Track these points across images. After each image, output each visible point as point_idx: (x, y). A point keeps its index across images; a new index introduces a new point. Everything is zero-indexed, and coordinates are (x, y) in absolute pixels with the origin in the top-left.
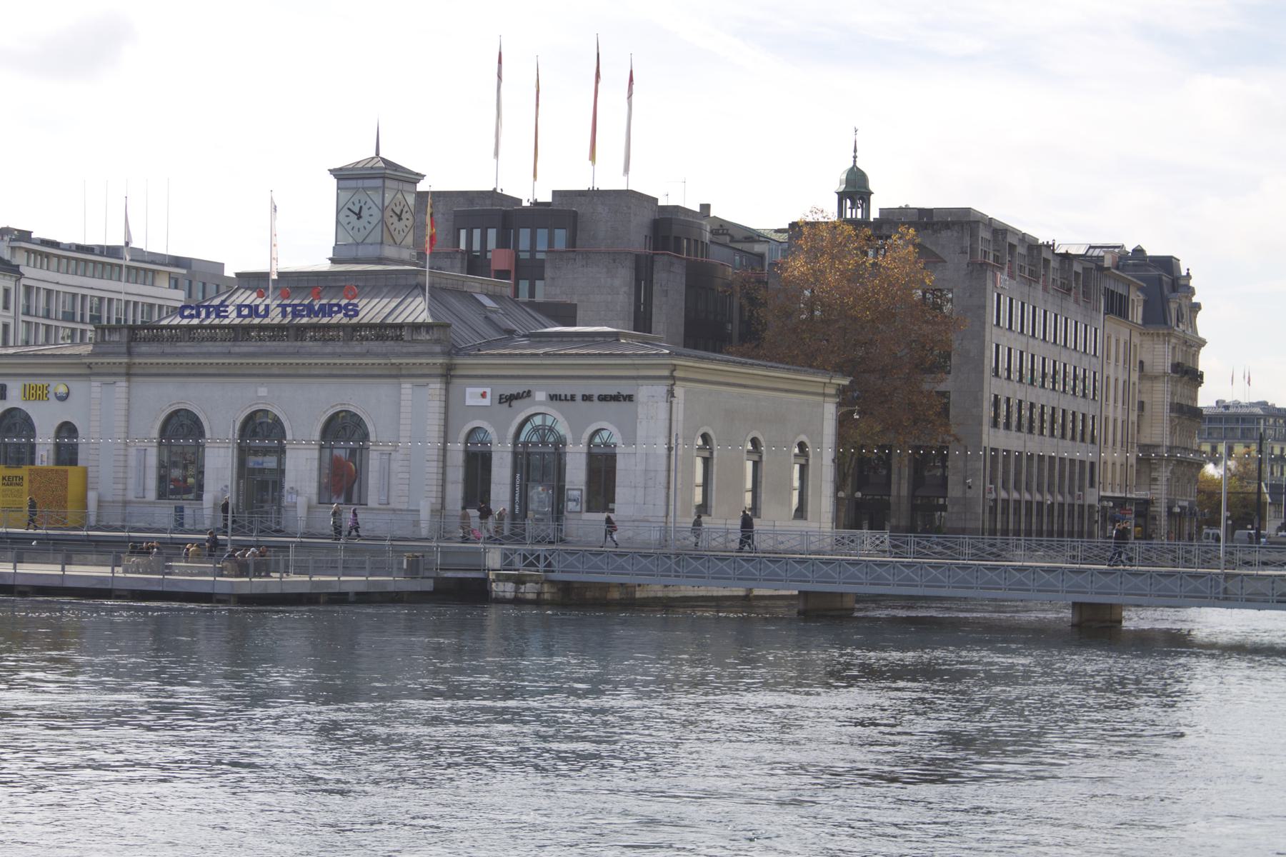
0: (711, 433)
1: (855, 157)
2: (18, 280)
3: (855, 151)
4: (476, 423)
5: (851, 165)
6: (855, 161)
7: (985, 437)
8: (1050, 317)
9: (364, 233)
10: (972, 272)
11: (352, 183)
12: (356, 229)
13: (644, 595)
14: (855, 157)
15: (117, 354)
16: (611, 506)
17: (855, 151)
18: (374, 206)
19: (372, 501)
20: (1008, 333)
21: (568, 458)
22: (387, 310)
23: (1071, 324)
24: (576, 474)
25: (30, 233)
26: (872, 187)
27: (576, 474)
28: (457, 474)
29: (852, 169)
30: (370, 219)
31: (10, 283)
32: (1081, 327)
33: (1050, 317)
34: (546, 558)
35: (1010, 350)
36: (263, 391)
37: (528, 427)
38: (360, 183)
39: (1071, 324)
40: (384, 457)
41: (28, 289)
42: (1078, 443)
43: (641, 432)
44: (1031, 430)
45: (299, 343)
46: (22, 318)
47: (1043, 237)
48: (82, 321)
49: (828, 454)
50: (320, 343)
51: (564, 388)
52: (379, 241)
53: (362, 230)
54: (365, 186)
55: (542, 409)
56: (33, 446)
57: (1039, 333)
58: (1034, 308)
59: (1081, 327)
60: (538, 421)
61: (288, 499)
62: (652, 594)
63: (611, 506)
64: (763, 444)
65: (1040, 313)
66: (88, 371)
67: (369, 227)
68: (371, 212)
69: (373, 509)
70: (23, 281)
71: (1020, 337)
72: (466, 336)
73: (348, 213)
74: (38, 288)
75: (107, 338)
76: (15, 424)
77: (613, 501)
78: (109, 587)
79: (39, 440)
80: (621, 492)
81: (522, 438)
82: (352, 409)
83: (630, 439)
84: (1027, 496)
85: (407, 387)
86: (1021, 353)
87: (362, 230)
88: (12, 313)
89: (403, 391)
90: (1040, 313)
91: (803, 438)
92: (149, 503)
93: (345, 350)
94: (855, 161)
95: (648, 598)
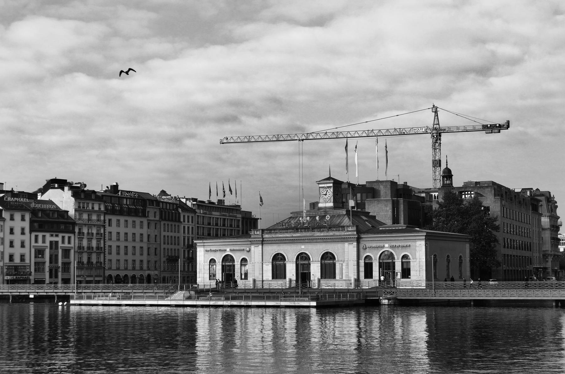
0: (450, 255)
1: (447, 165)
2: (195, 214)
3: (447, 163)
4: (368, 254)
5: (446, 167)
6: (447, 166)
7: (502, 251)
8: (517, 213)
10: (495, 201)
12: (325, 199)
14: (447, 165)
15: (259, 238)
16: (409, 277)
17: (447, 163)
18: (330, 192)
19: (338, 277)
20: (506, 219)
21: (396, 263)
23: (523, 215)
24: (398, 268)
26: (452, 174)
27: (398, 268)
28: (362, 269)
29: (446, 168)
30: (330, 195)
31: (193, 215)
32: (525, 215)
33: (517, 213)
34: (396, 293)
35: (507, 224)
36: (303, 247)
37: (383, 255)
39: (523, 215)
40: (341, 265)
41: (198, 216)
42: (527, 251)
43: (417, 254)
44: (528, 250)
45: (313, 233)
46: (197, 225)
47: (511, 188)
48: (213, 225)
49: (468, 259)
50: (319, 232)
51: (394, 244)
53: (327, 198)
55: (387, 249)
56: (234, 266)
57: (515, 218)
58: (513, 211)
59: (525, 215)
60: (386, 253)
61: (312, 278)
63: (409, 277)
64: (463, 257)
65: (514, 212)
66: (250, 243)
68: (329, 193)
69: (337, 280)
70: (197, 214)
71: (510, 220)
72: (535, 249)
74: (201, 216)
75: (255, 233)
76: (228, 259)
77: (410, 275)
78: (279, 305)
79: (236, 263)
80: (412, 273)
81: (381, 258)
82: (330, 251)
83: (415, 258)
84: (514, 268)
85: (346, 244)
86: (510, 224)
87: (327, 198)
88: (194, 224)
89: (345, 246)
90: (514, 212)
91: (461, 254)
92: (270, 280)
93: (327, 234)
94: (447, 166)
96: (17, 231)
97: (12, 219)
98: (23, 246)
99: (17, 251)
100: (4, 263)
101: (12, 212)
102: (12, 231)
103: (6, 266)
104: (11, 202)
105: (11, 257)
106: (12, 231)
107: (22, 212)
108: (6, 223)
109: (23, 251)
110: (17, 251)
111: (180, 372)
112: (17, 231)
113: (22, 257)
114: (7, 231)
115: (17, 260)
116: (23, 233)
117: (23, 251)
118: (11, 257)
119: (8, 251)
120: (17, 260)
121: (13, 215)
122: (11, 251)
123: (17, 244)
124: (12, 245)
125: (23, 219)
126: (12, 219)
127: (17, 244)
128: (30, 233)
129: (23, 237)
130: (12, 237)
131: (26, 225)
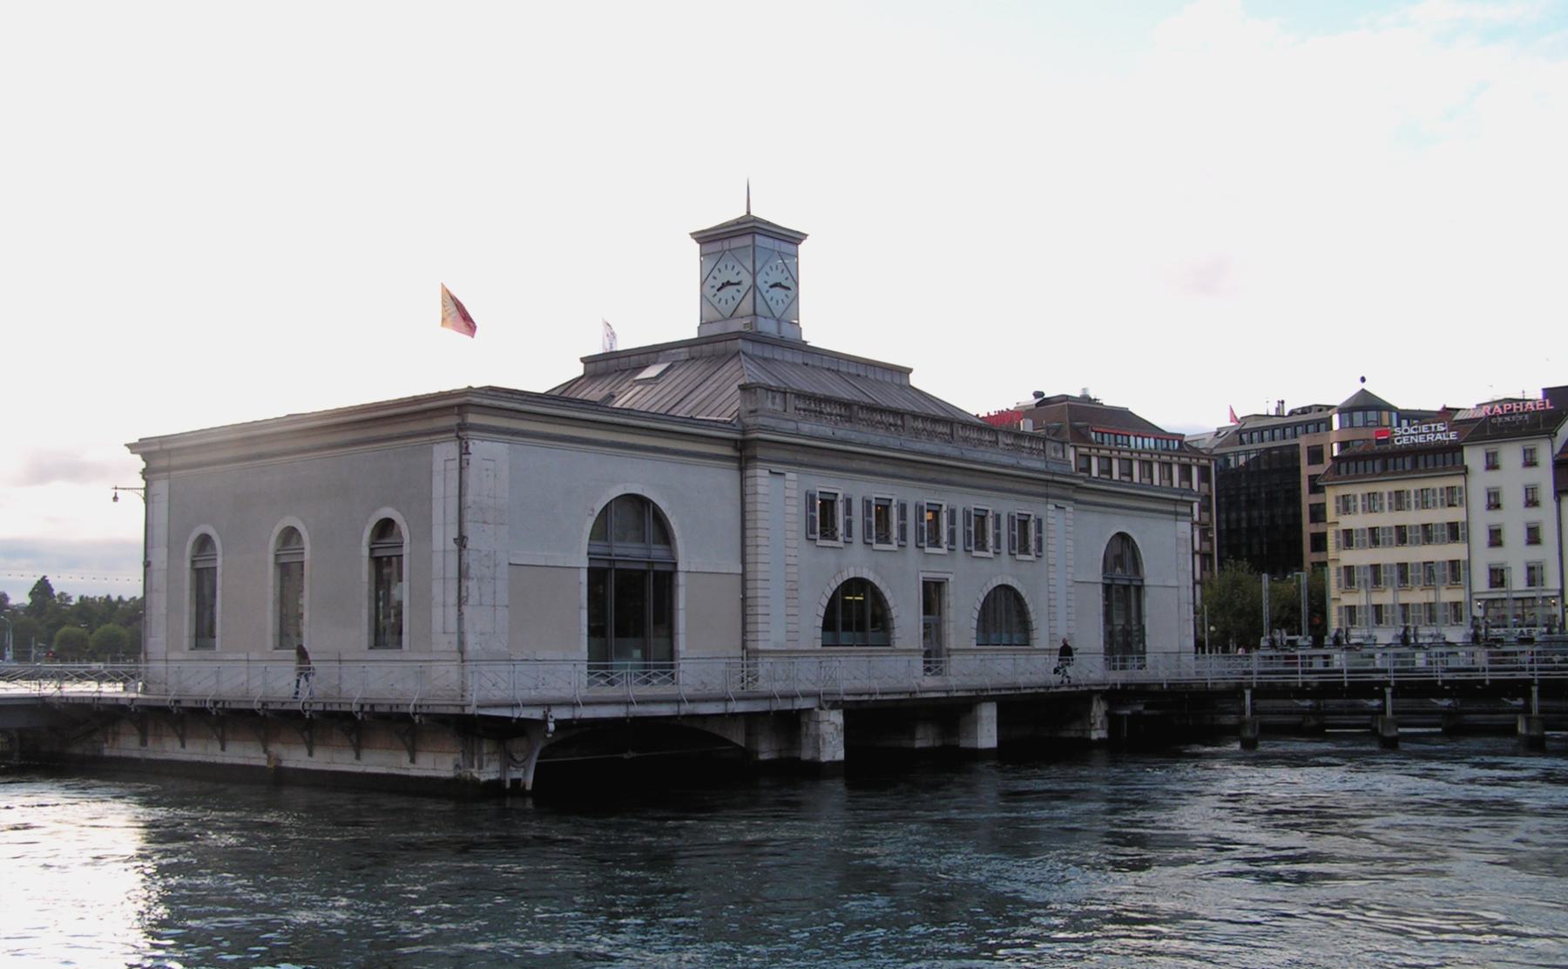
9: (732, 304)
11: (716, 247)
13: (115, 753)
22: (652, 402)
25: (906, 372)
38: (726, 244)
52: (751, 311)
54: (732, 247)
62: (124, 753)
67: (739, 297)
73: (714, 287)
95: (120, 757)
96: (1513, 498)
97: (1492, 465)
98: (1533, 536)
99: (1515, 556)
100: (1471, 595)
101: (1491, 448)
102: (1494, 503)
103: (1479, 600)
104: (1493, 416)
105: (1497, 577)
106: (1494, 503)
107: (1487, 446)
108: (1472, 480)
109: (1534, 554)
110: (1515, 556)
111: (1135, 966)
112: (1513, 498)
113: (1534, 574)
114: (1478, 500)
115: (1518, 582)
116: (1532, 502)
117: (1534, 554)
118: (1497, 577)
119: (1482, 558)
120: (1518, 582)
121: (1495, 454)
122: (1497, 556)
123: (1514, 535)
124: (1495, 538)
125: (1530, 462)
126: (1492, 465)
127: (1514, 535)
128: (1559, 501)
129: (1533, 515)
130: (1495, 518)
131: (1543, 476)
